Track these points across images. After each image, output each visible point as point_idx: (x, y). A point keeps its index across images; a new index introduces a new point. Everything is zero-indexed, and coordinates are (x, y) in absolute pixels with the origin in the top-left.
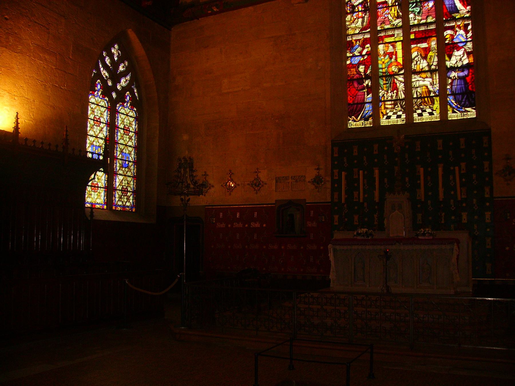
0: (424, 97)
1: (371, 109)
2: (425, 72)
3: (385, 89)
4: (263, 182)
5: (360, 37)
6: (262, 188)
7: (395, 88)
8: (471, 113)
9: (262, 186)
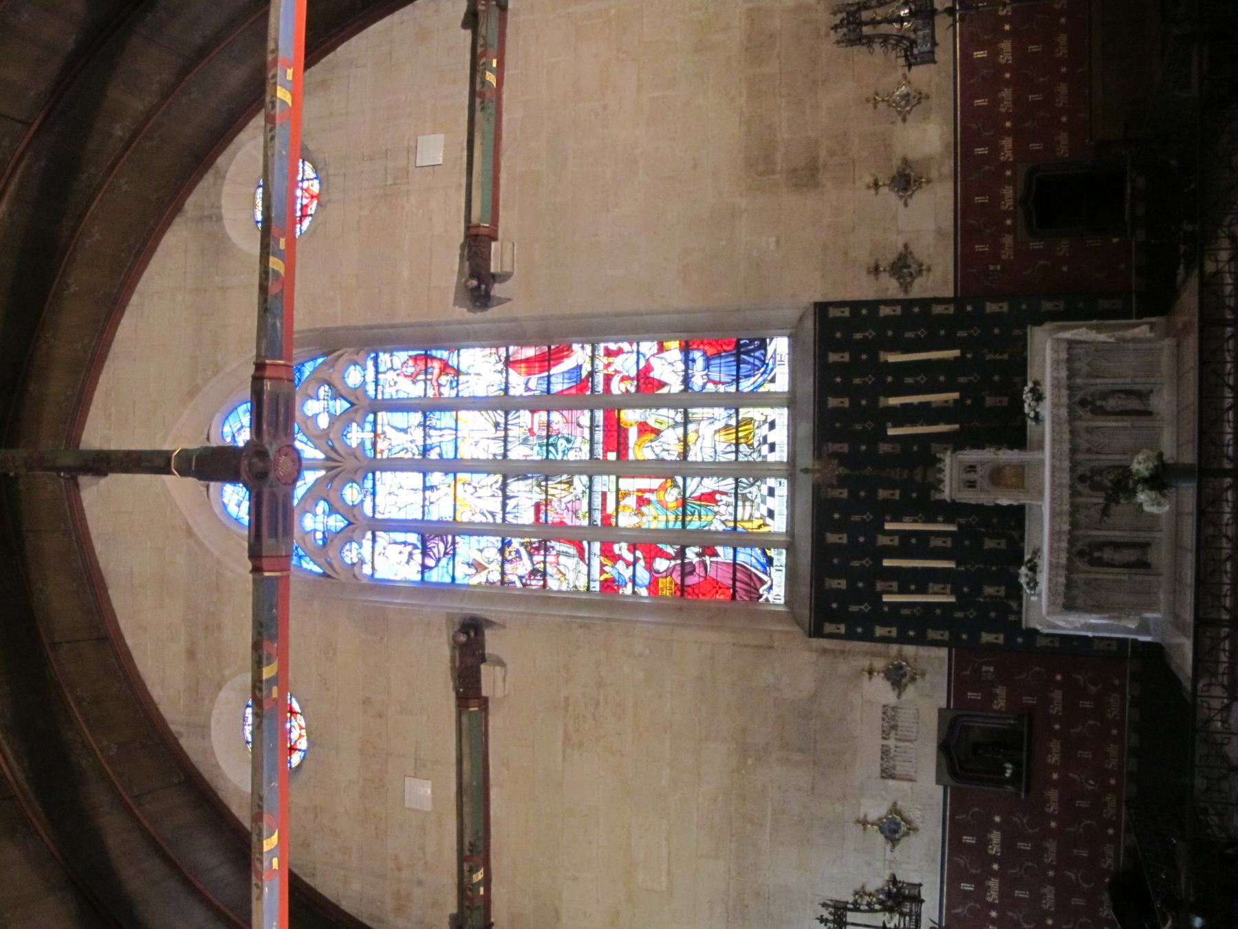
0: (737, 438)
1: (748, 550)
2: (686, 434)
3: (710, 518)
4: (891, 812)
5: (596, 562)
6: (906, 814)
7: (710, 497)
8: (780, 346)
9: (899, 813)
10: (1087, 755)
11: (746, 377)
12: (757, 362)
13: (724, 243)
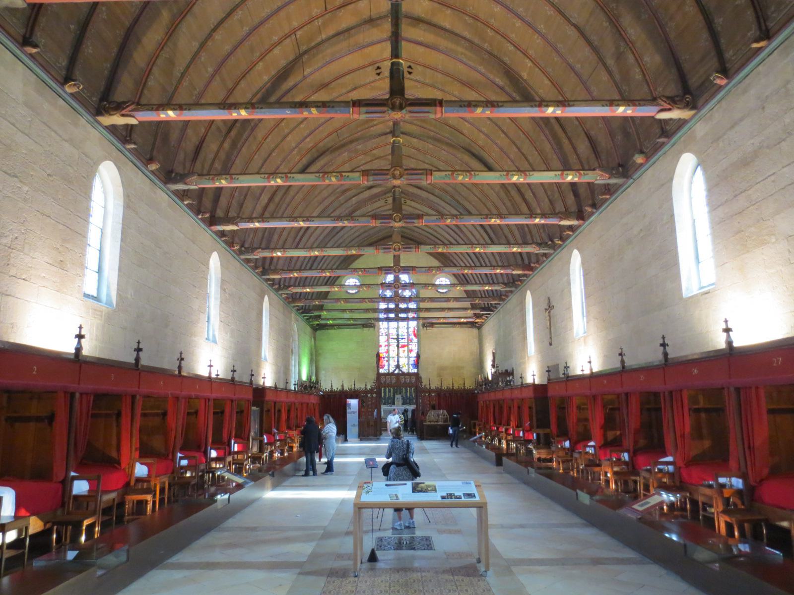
8: (416, 371)
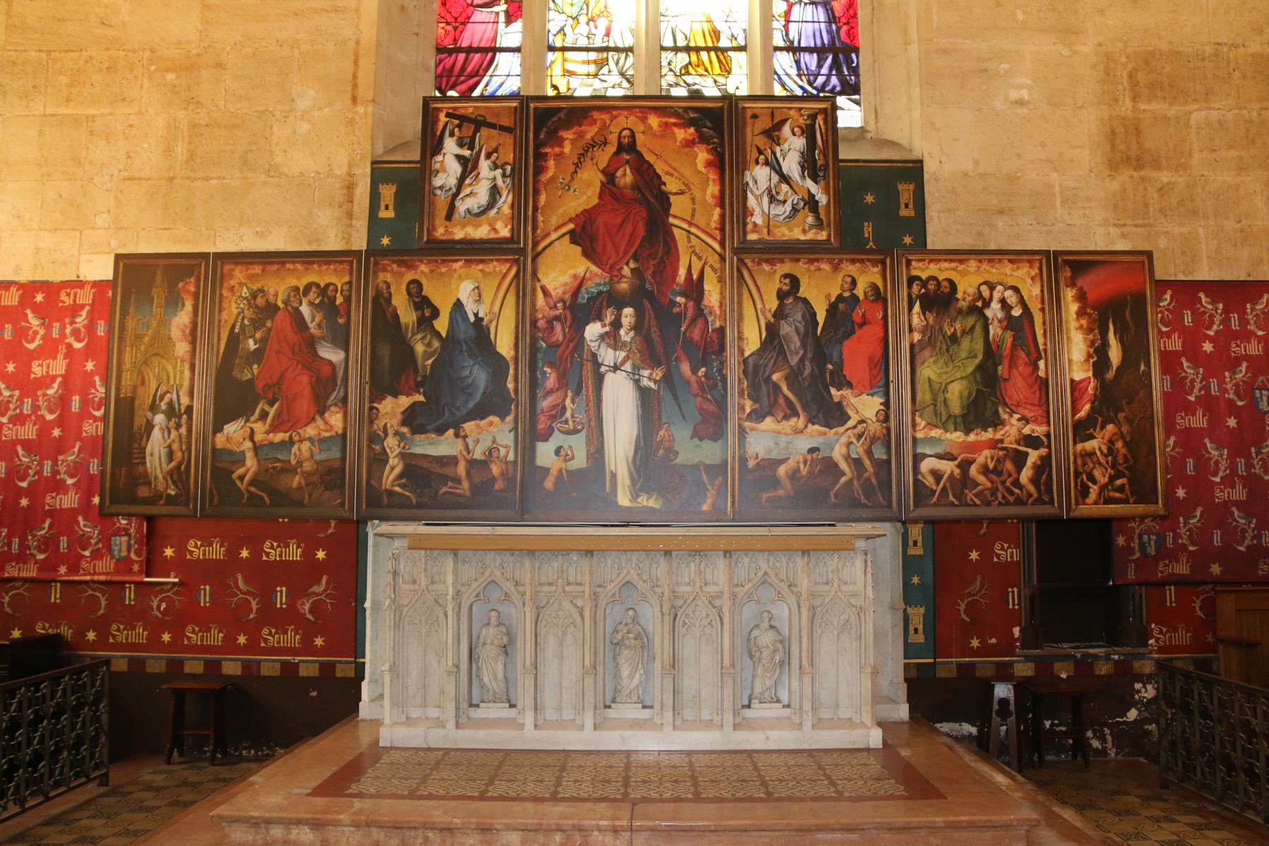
0: (698, 50)
1: (517, 70)
10: (205, 596)
11: (798, 62)
12: (821, 80)
13: (1020, 15)
